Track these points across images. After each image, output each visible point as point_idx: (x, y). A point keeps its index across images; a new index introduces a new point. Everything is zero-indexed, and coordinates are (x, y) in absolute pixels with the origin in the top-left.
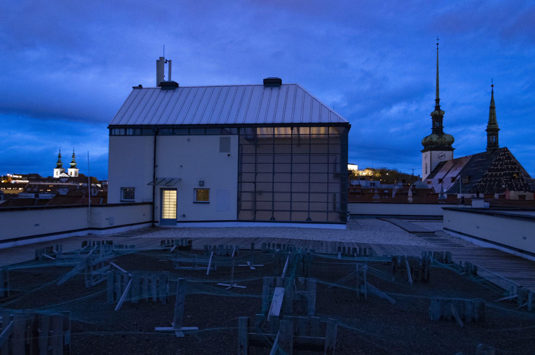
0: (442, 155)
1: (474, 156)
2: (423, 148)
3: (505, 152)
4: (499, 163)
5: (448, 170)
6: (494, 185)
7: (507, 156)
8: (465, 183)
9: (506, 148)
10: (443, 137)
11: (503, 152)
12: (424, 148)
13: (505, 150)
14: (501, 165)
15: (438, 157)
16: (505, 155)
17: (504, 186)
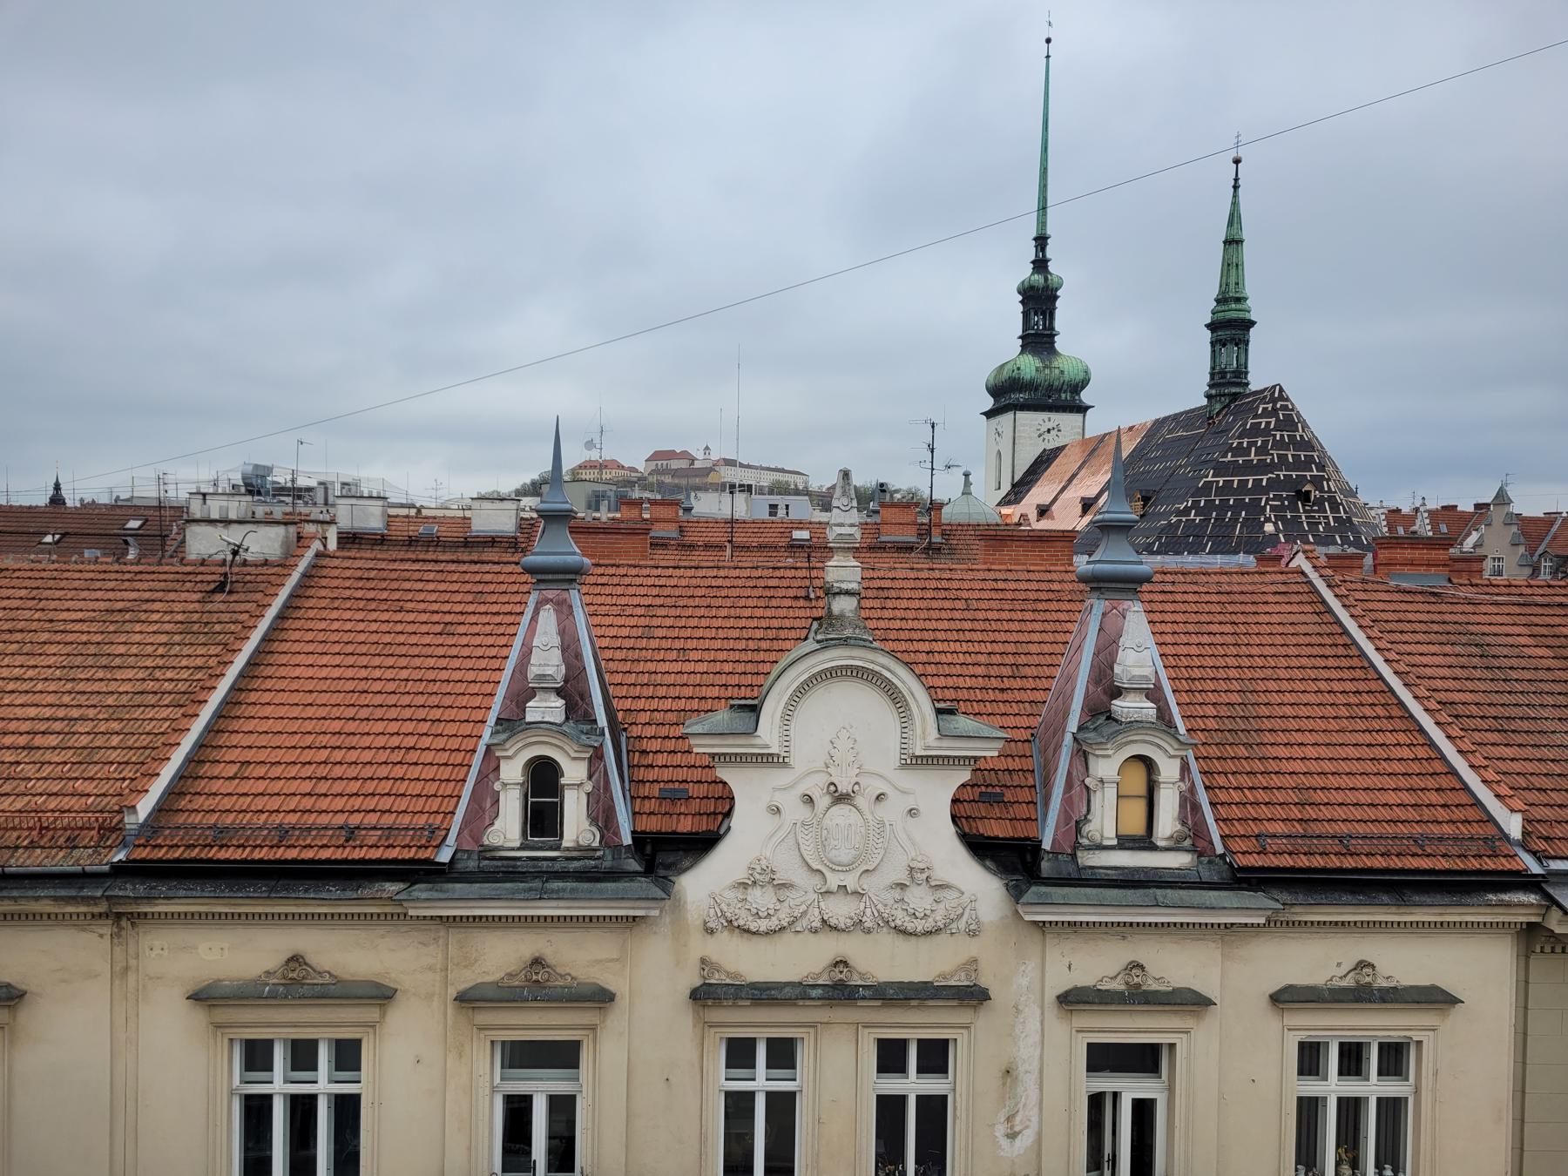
1: (1159, 424)
2: (988, 403)
3: (1274, 401)
5: (1066, 479)
6: (1235, 520)
10: (1055, 364)
11: (1268, 403)
13: (1276, 395)
14: (1262, 450)
17: (1269, 528)
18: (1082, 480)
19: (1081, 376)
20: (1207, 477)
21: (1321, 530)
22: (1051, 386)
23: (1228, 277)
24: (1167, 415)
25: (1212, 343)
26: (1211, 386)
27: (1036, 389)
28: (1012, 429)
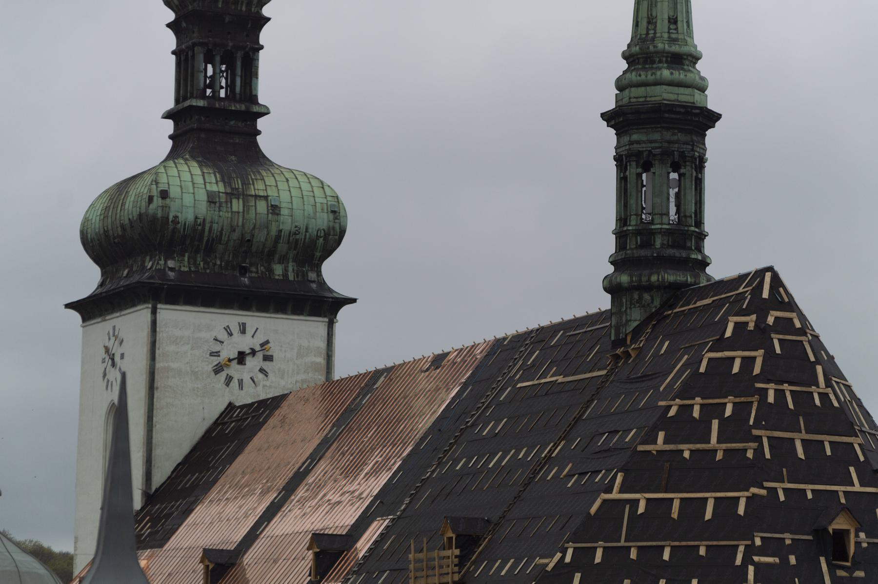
0: (245, 343)
3: (760, 307)
4: (712, 411)
9: (768, 276)
10: (258, 188)
11: (746, 313)
13: (766, 294)
15: (209, 368)
18: (320, 487)
19: (323, 221)
20: (609, 490)
22: (246, 244)
24: (522, 329)
25: (618, 159)
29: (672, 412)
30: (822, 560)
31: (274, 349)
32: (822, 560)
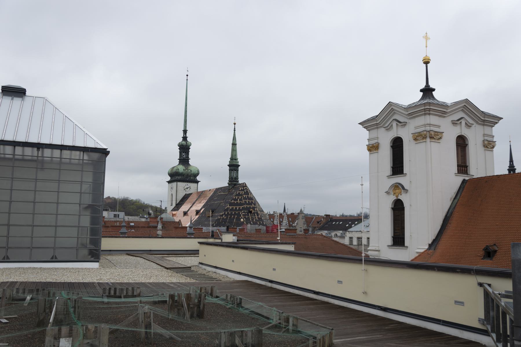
0: (187, 186)
1: (217, 190)
2: (169, 178)
3: (243, 187)
4: (238, 198)
6: (234, 218)
7: (245, 191)
8: (209, 216)
10: (189, 168)
12: (170, 179)
13: (244, 185)
16: (243, 190)
21: (254, 220)
22: (188, 175)
23: (233, 153)
25: (229, 170)
26: (229, 181)
27: (183, 176)
28: (176, 187)
29: (234, 198)
30: (249, 214)
31: (191, 187)
32: (249, 214)
